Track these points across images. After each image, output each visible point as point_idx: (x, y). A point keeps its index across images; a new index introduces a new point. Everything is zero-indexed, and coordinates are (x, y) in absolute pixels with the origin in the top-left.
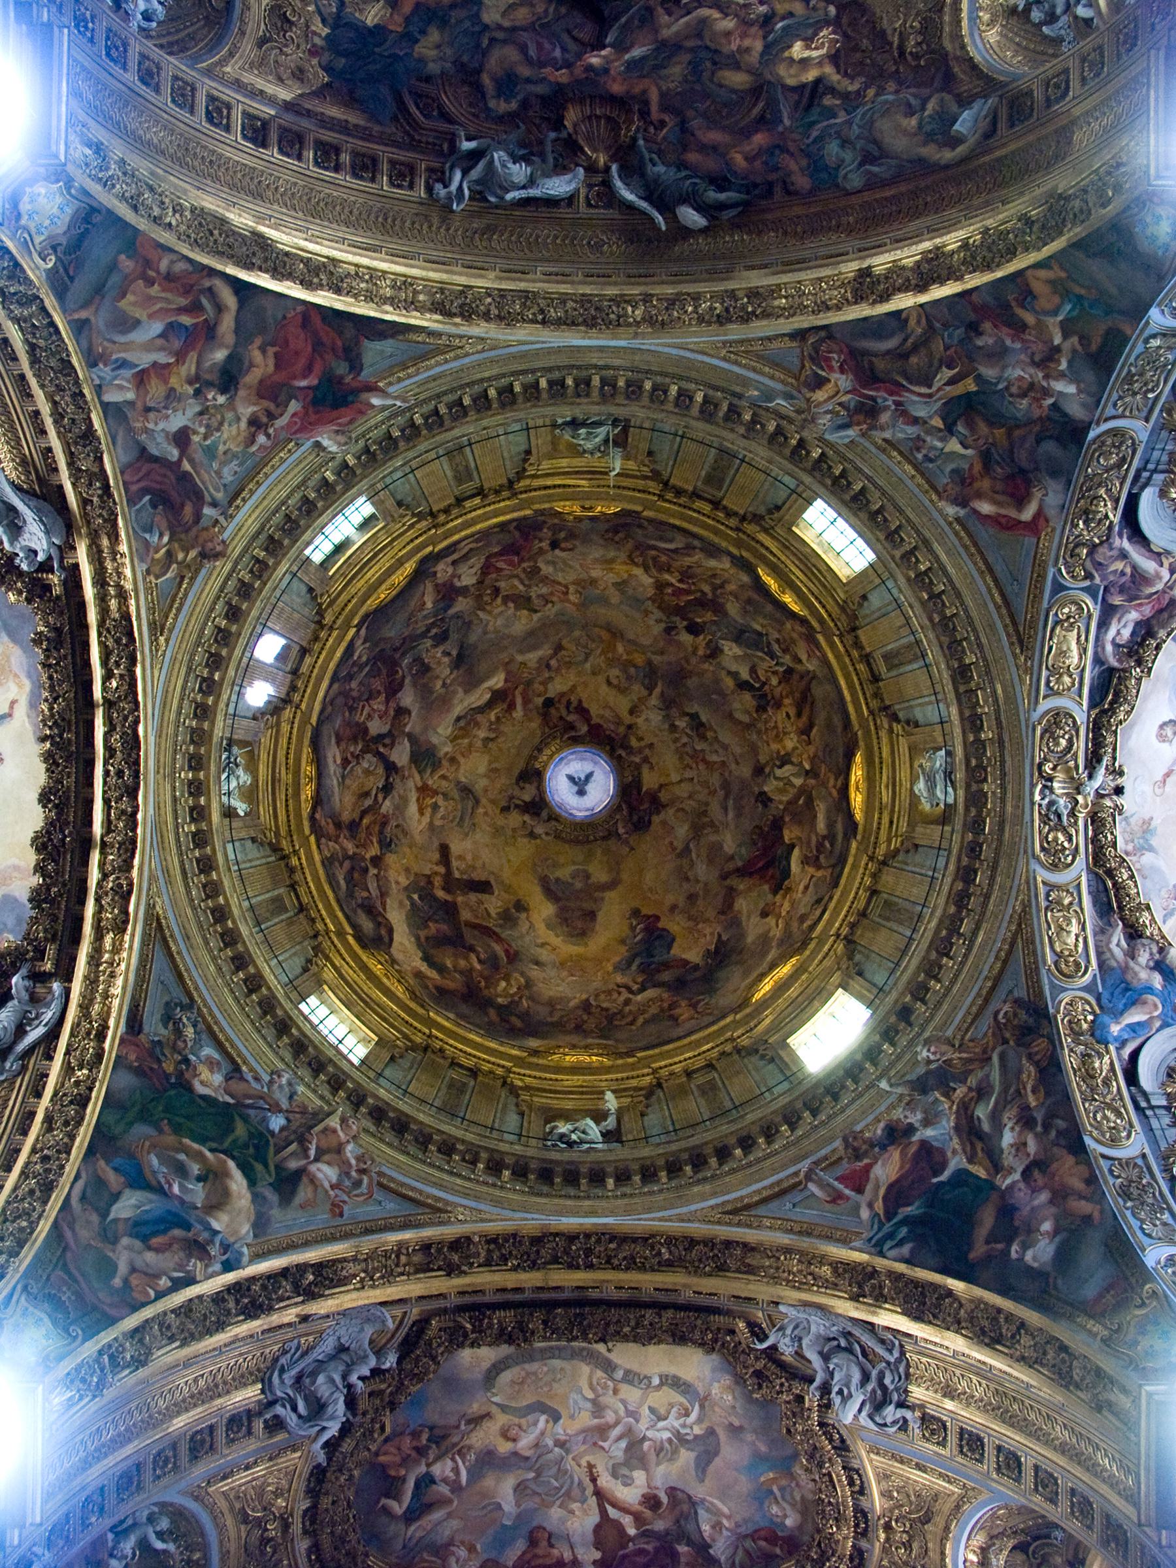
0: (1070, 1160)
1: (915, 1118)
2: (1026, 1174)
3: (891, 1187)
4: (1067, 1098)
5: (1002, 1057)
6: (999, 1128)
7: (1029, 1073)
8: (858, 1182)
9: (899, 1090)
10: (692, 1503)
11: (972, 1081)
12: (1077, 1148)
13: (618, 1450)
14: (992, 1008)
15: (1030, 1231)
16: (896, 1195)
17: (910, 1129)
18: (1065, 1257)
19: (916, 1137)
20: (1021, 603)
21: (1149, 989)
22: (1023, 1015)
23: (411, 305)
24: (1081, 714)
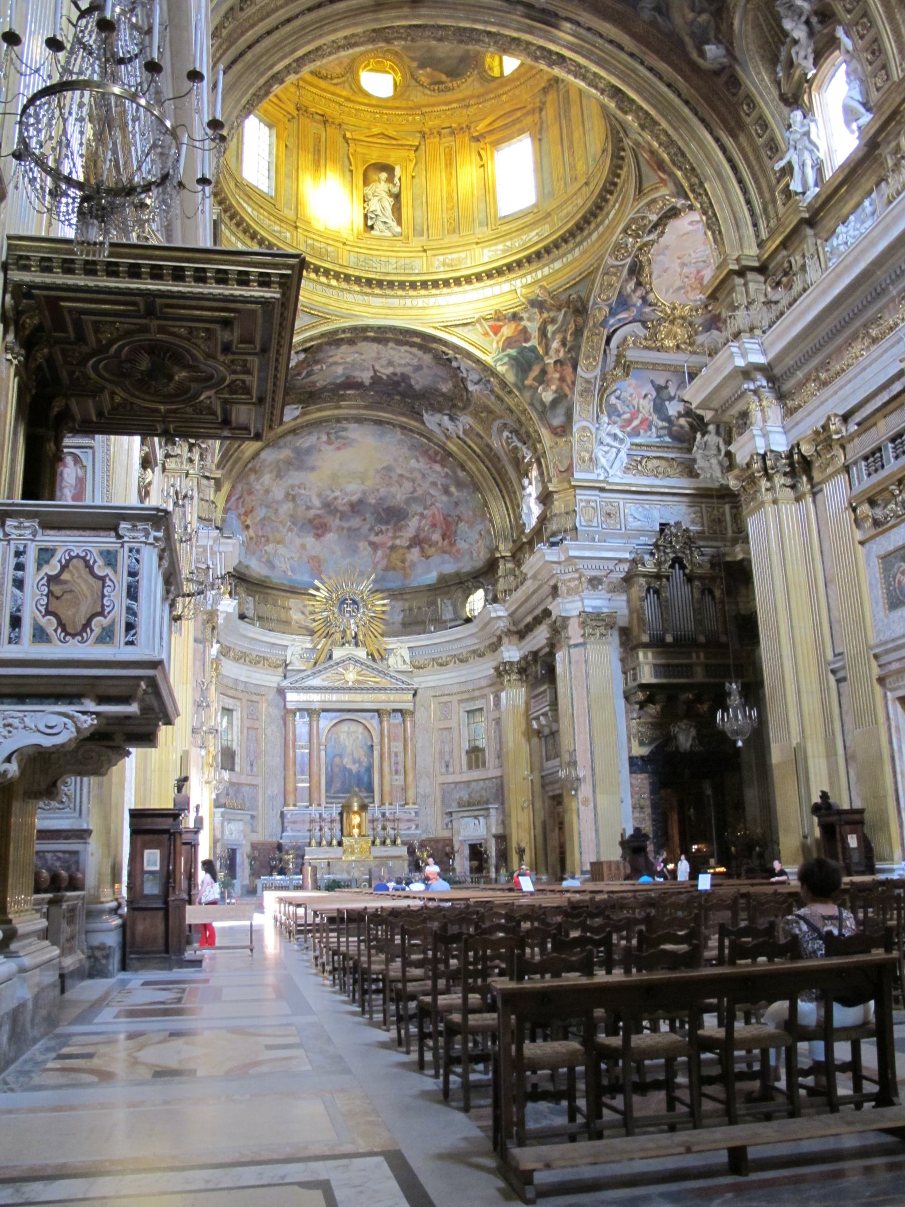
0: (570, 370)
1: (525, 315)
2: (556, 362)
3: (507, 338)
4: (579, 348)
5: (566, 313)
6: (554, 339)
7: (572, 326)
8: (496, 330)
9: (523, 300)
10: (409, 378)
11: (552, 314)
12: (575, 368)
13: (384, 363)
14: (569, 292)
15: (548, 385)
16: (509, 343)
17: (521, 319)
18: (555, 403)
19: (523, 323)
20: (646, 185)
21: (634, 305)
22: (579, 304)
23: (356, 45)
24: (654, 218)
